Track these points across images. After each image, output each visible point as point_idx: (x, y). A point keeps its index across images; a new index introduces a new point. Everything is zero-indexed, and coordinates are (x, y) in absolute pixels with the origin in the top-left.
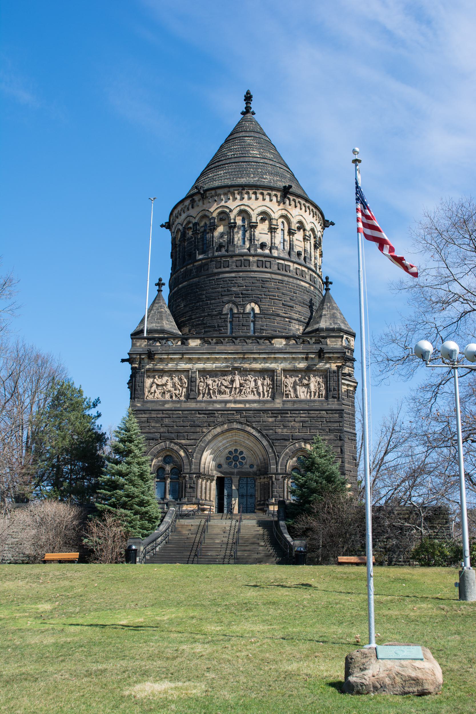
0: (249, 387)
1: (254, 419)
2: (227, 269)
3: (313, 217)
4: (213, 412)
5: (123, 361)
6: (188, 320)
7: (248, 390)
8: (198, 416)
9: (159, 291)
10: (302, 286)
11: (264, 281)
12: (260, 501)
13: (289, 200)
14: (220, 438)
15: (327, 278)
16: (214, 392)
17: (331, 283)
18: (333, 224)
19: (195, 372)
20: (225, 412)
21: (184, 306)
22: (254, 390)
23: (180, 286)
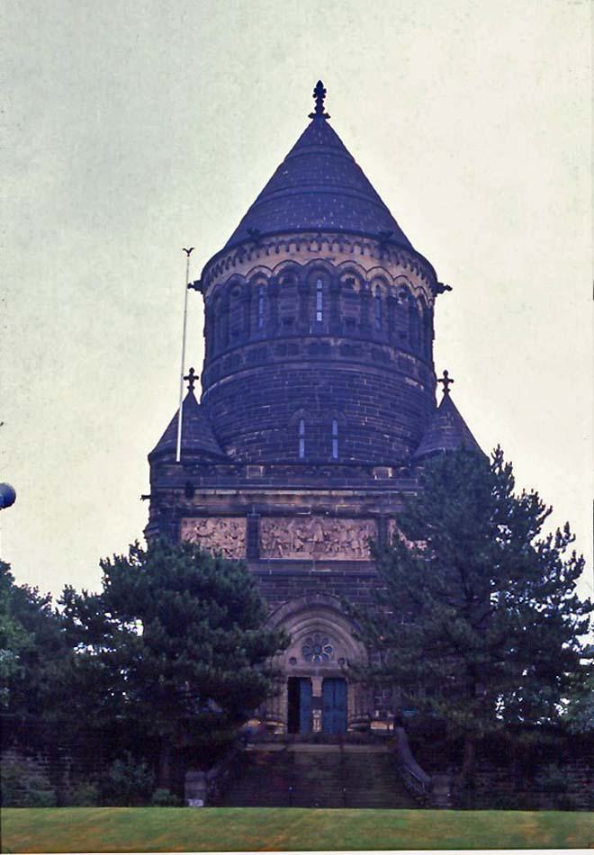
2: (295, 357)
3: (422, 279)
4: (284, 578)
5: (144, 497)
6: (235, 435)
9: (191, 388)
10: (408, 385)
11: (353, 376)
12: (355, 716)
13: (388, 253)
14: (294, 620)
15: (446, 373)
16: (284, 548)
17: (452, 381)
18: (449, 289)
21: (230, 414)
22: (346, 545)
23: (222, 381)
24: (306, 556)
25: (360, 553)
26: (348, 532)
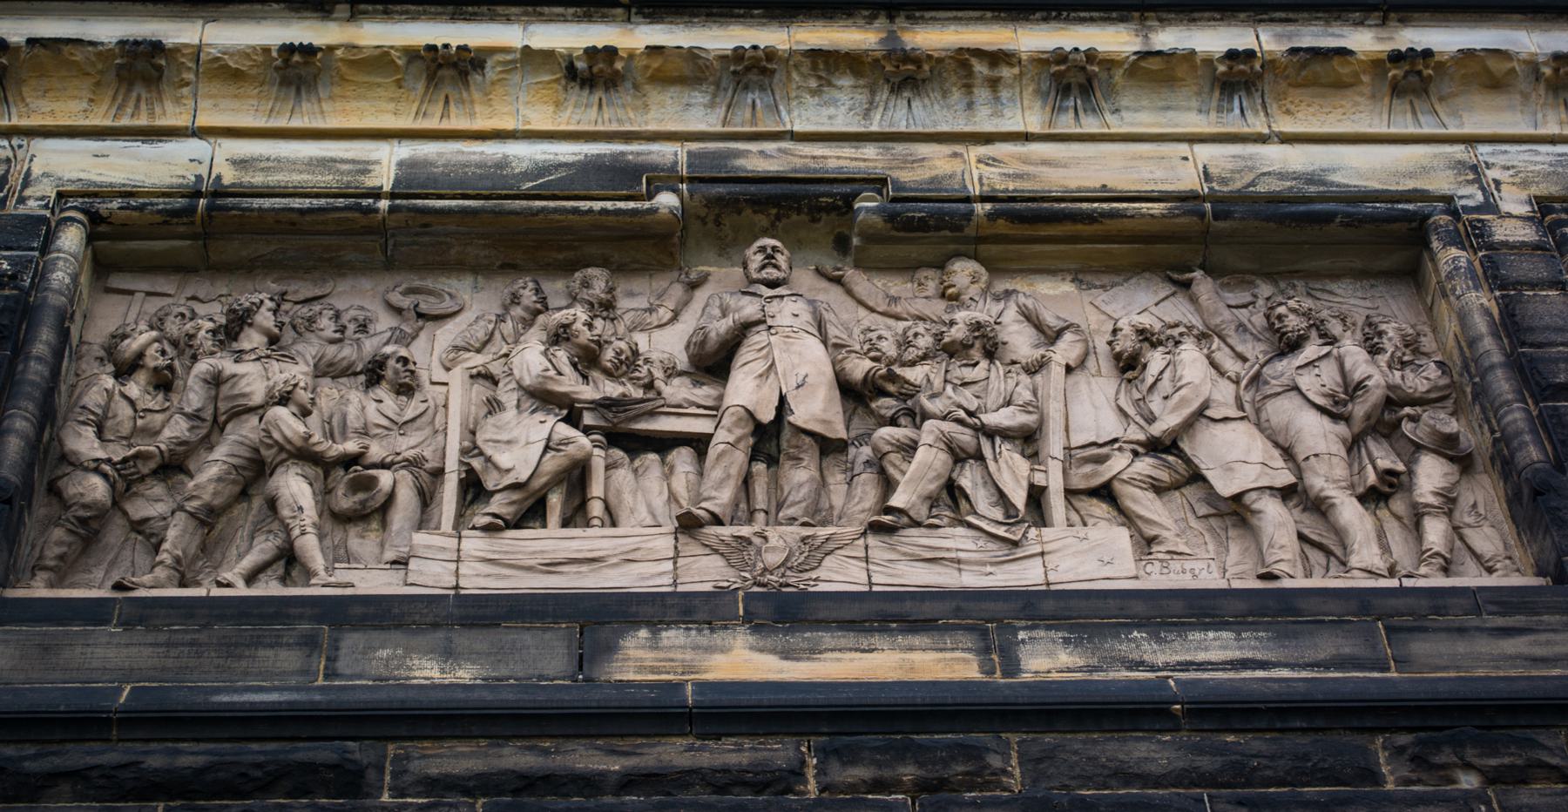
0: (1028, 439)
7: (1023, 465)
19: (41, 231)
25: (1326, 543)
26: (1128, 365)
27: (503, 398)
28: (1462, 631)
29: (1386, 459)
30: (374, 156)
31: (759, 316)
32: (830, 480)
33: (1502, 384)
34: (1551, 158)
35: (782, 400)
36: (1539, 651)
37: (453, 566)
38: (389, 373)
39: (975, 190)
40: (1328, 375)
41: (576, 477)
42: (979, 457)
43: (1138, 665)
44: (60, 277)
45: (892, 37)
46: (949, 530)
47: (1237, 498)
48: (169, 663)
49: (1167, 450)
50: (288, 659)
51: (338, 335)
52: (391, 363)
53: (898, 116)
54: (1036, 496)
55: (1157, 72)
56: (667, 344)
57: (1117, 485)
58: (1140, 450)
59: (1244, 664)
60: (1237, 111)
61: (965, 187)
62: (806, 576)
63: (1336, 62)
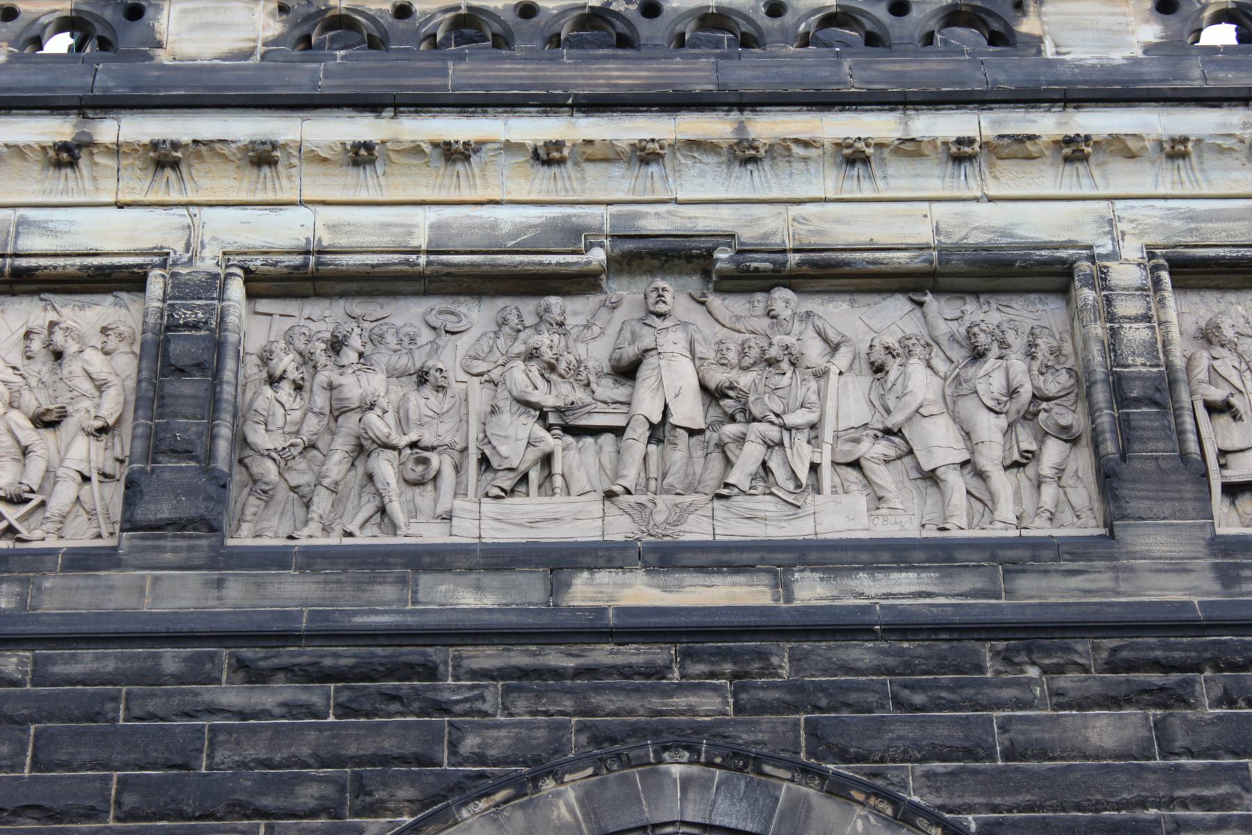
1: (903, 730)
4: (410, 654)
7: (807, 449)
8: (232, 695)
20: (555, 657)
24: (571, 518)
25: (984, 501)
26: (878, 369)
27: (501, 404)
28: (1046, 572)
29: (1028, 444)
30: (414, 221)
31: (653, 345)
32: (694, 455)
33: (1101, 395)
34: (1163, 212)
35: (666, 406)
36: (1088, 586)
37: (477, 522)
38: (431, 378)
39: (789, 245)
40: (998, 383)
41: (547, 460)
42: (781, 444)
43: (861, 595)
44: (232, 319)
45: (741, 128)
46: (761, 497)
47: (933, 471)
48: (327, 594)
49: (895, 434)
50: (388, 591)
51: (398, 347)
52: (432, 372)
53: (744, 184)
54: (814, 468)
55: (910, 149)
56: (597, 353)
57: (863, 462)
58: (880, 434)
59: (921, 594)
60: (963, 177)
61: (784, 242)
62: (677, 528)
63: (1028, 144)
